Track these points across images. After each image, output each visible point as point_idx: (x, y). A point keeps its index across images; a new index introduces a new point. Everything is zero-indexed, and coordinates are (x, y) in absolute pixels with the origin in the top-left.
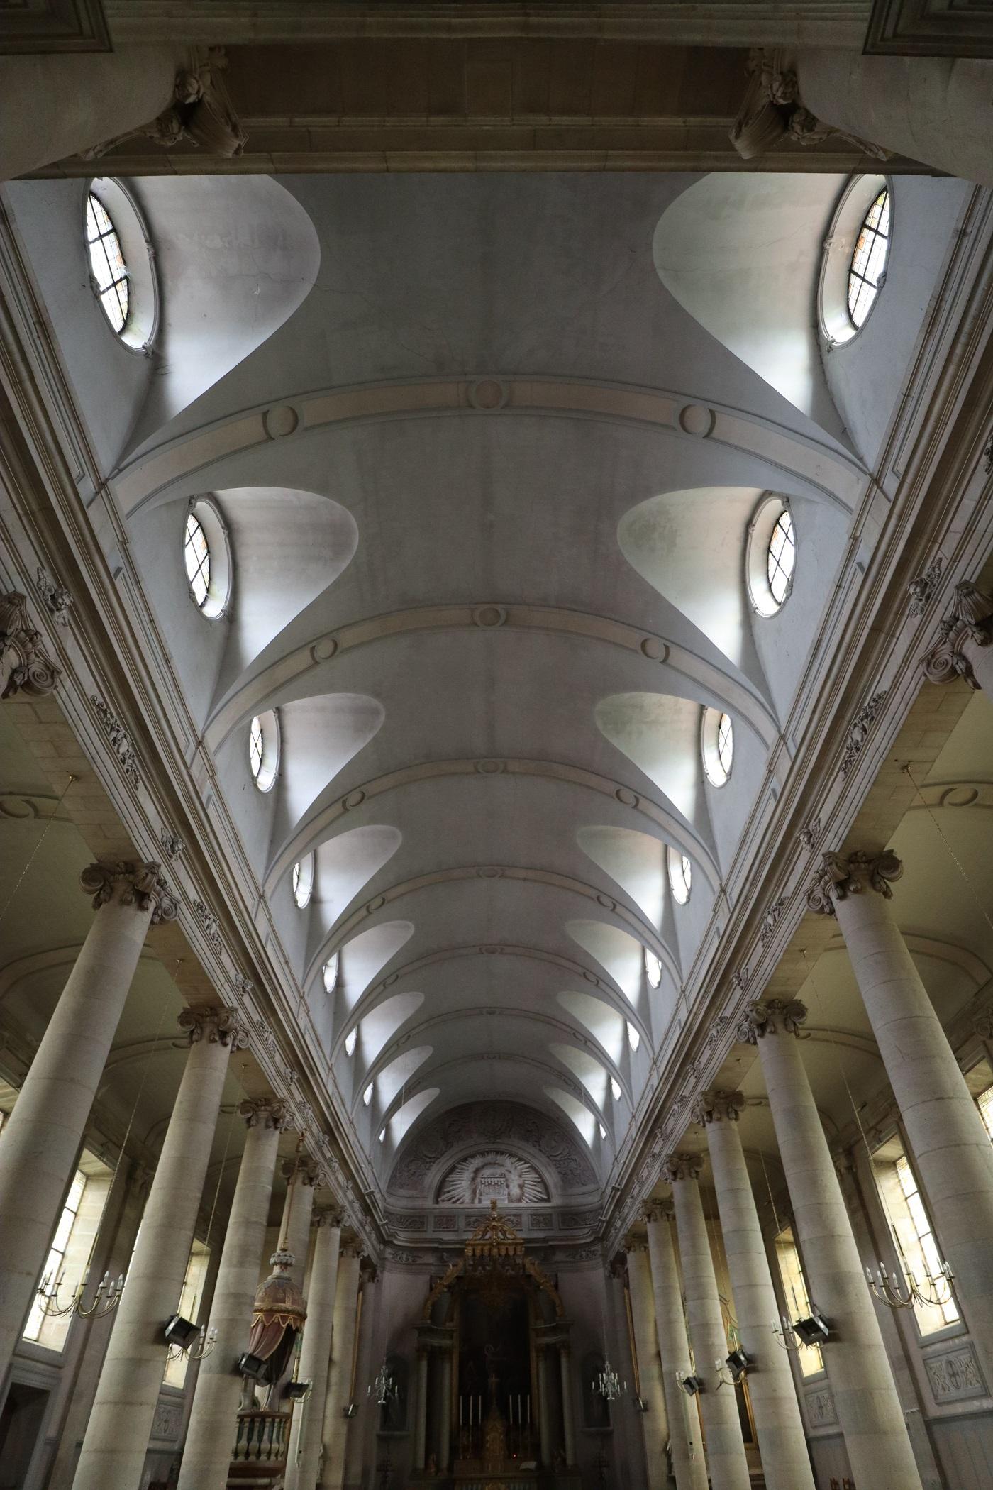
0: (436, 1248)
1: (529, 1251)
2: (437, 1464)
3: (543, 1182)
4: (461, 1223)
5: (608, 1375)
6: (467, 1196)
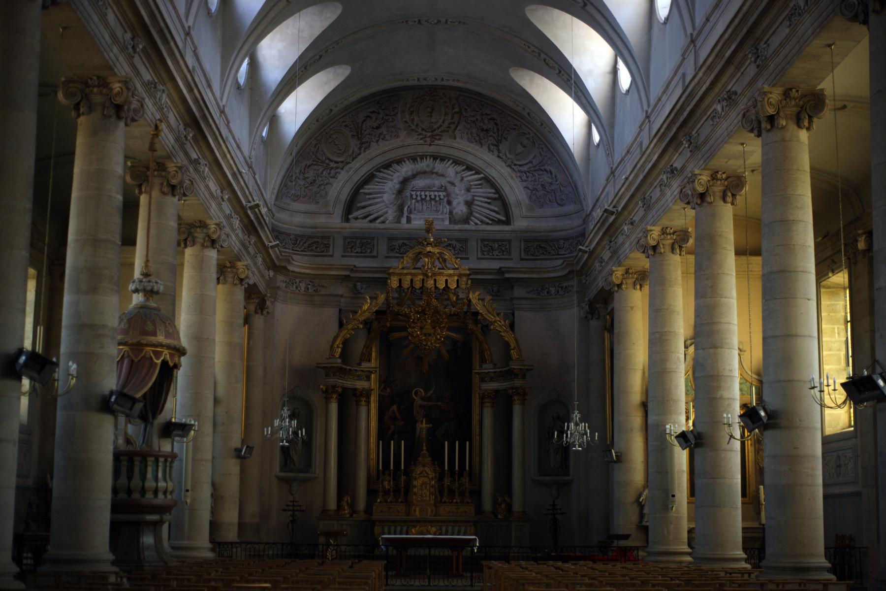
0: (347, 277)
1: (476, 284)
2: (353, 507)
3: (500, 199)
4: (382, 248)
5: (577, 425)
6: (391, 215)
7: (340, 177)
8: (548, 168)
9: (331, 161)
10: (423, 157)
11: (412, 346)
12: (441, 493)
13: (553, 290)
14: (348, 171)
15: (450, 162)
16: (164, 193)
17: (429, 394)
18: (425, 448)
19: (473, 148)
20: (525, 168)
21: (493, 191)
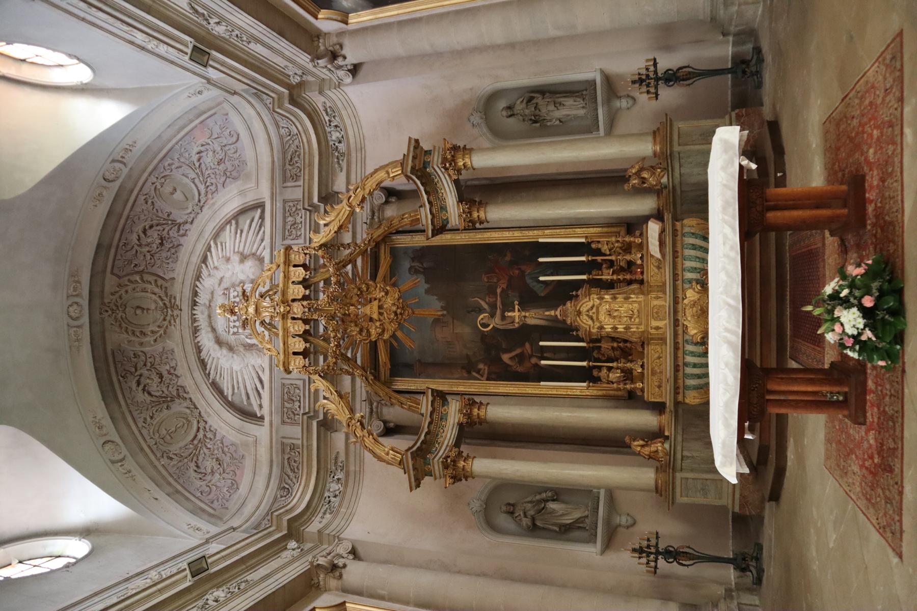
7: (215, 426)
8: (195, 158)
9: (196, 436)
10: (195, 321)
11: (399, 334)
12: (630, 283)
13: (335, 135)
14: (209, 415)
15: (197, 283)
17: (486, 306)
18: (552, 313)
19: (183, 254)
20: (202, 188)
21: (228, 227)
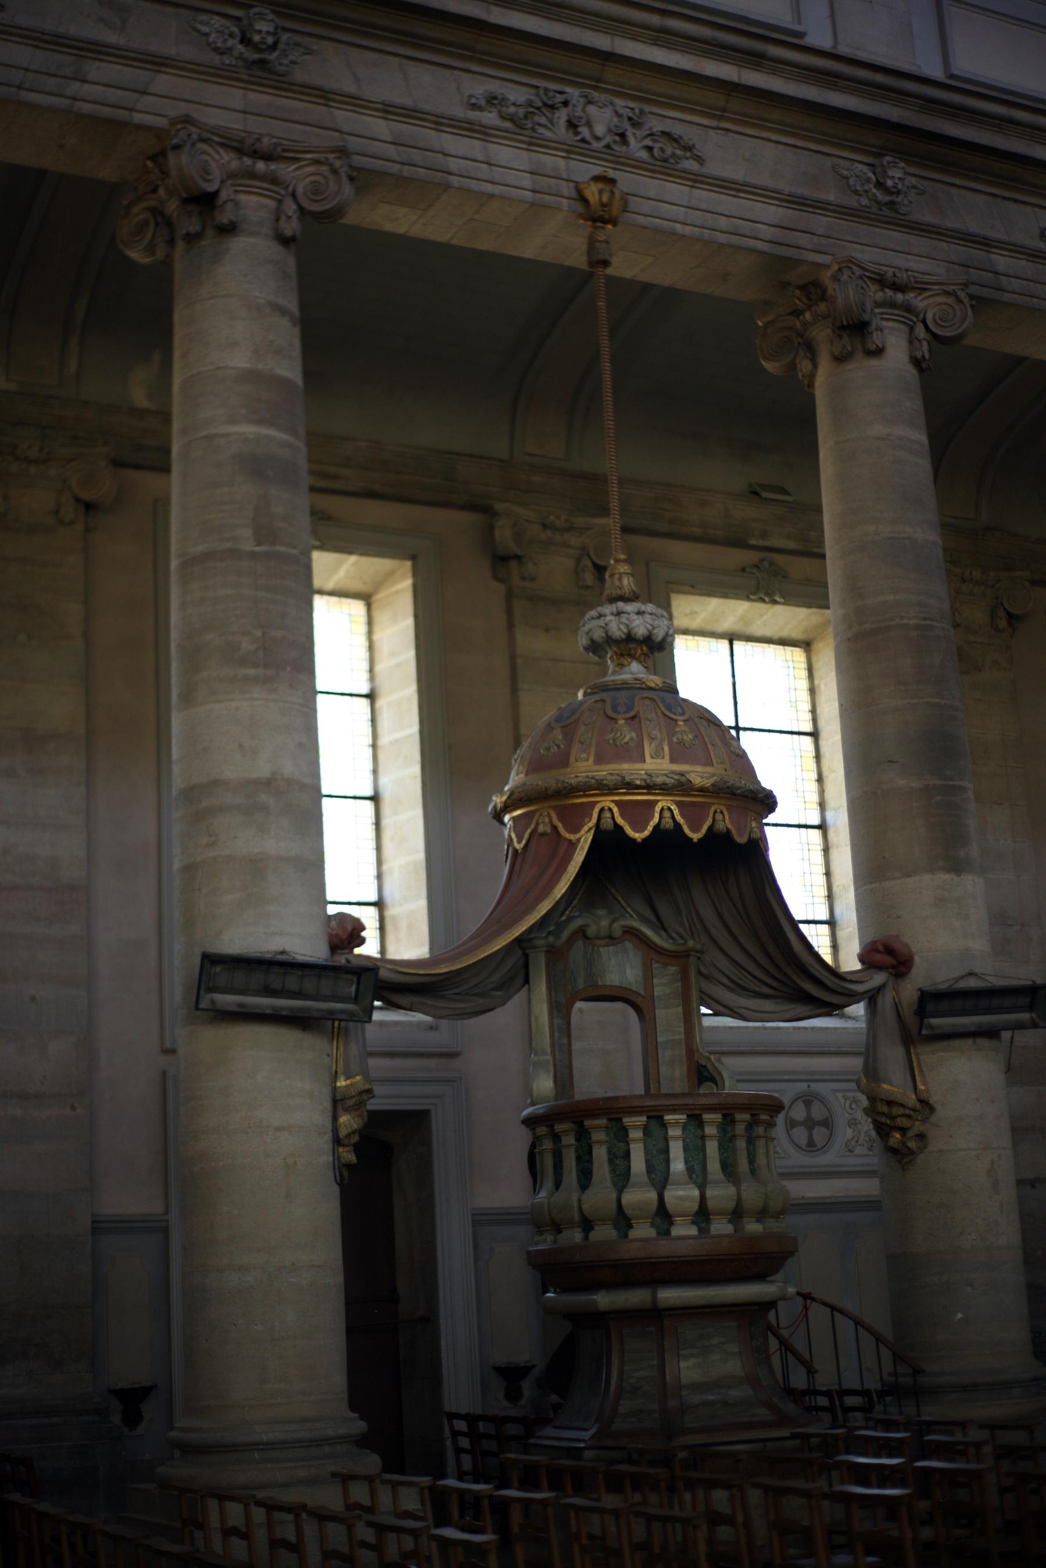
16: (841, 359)
